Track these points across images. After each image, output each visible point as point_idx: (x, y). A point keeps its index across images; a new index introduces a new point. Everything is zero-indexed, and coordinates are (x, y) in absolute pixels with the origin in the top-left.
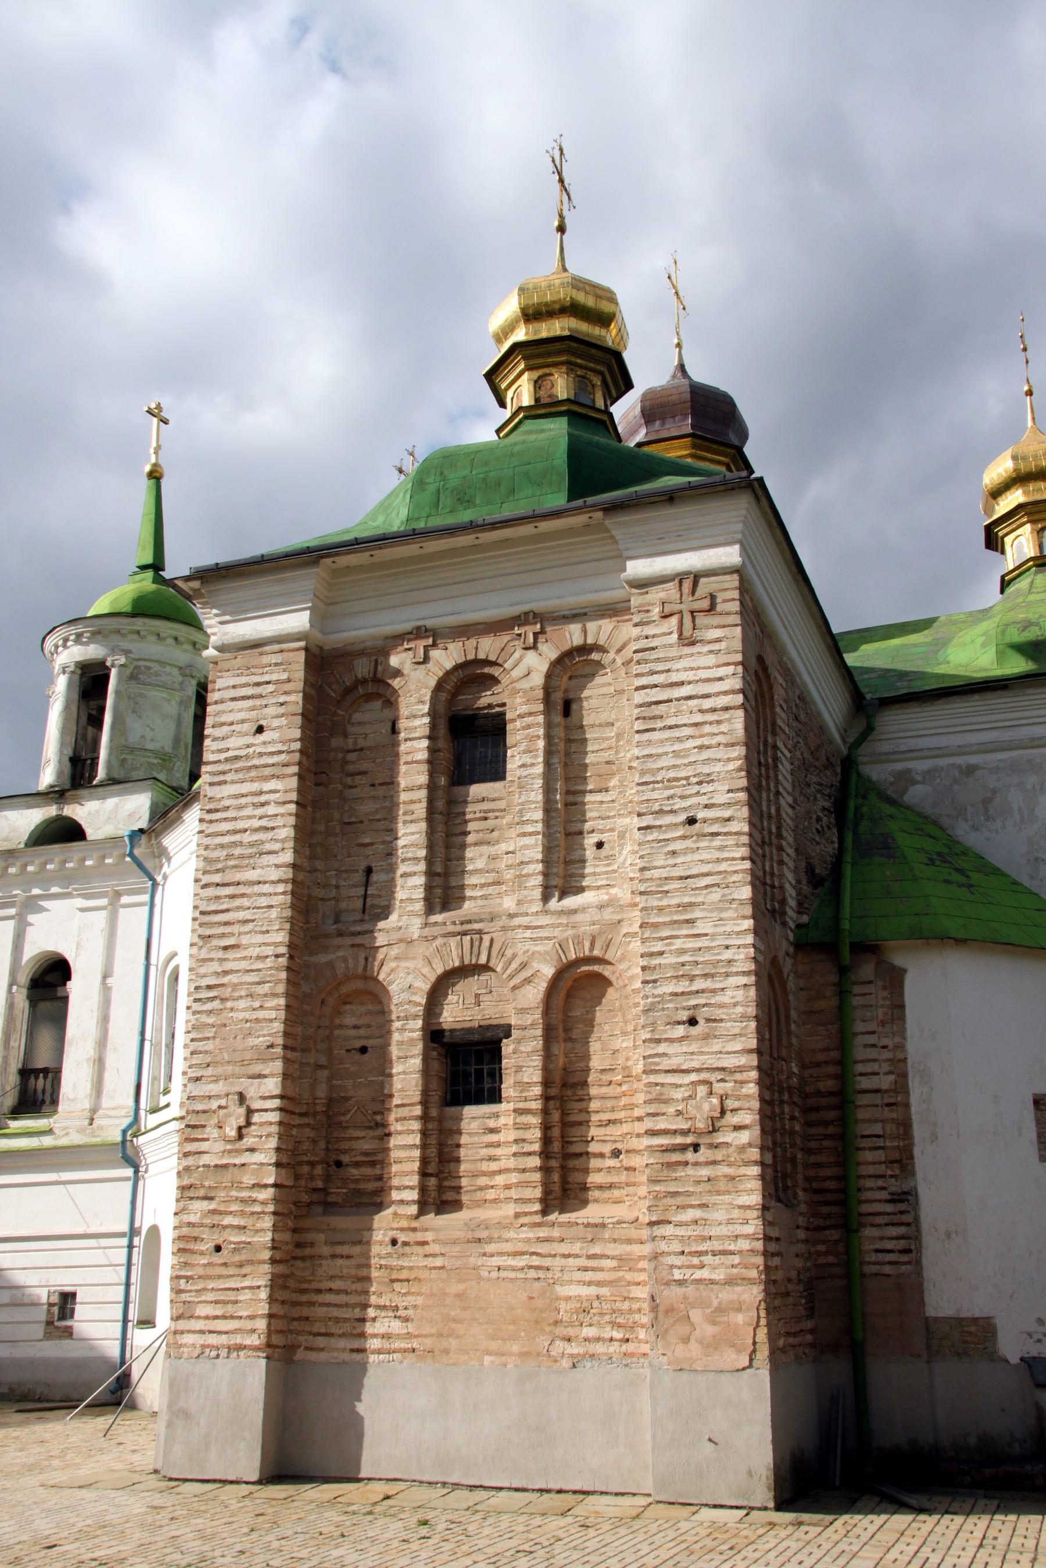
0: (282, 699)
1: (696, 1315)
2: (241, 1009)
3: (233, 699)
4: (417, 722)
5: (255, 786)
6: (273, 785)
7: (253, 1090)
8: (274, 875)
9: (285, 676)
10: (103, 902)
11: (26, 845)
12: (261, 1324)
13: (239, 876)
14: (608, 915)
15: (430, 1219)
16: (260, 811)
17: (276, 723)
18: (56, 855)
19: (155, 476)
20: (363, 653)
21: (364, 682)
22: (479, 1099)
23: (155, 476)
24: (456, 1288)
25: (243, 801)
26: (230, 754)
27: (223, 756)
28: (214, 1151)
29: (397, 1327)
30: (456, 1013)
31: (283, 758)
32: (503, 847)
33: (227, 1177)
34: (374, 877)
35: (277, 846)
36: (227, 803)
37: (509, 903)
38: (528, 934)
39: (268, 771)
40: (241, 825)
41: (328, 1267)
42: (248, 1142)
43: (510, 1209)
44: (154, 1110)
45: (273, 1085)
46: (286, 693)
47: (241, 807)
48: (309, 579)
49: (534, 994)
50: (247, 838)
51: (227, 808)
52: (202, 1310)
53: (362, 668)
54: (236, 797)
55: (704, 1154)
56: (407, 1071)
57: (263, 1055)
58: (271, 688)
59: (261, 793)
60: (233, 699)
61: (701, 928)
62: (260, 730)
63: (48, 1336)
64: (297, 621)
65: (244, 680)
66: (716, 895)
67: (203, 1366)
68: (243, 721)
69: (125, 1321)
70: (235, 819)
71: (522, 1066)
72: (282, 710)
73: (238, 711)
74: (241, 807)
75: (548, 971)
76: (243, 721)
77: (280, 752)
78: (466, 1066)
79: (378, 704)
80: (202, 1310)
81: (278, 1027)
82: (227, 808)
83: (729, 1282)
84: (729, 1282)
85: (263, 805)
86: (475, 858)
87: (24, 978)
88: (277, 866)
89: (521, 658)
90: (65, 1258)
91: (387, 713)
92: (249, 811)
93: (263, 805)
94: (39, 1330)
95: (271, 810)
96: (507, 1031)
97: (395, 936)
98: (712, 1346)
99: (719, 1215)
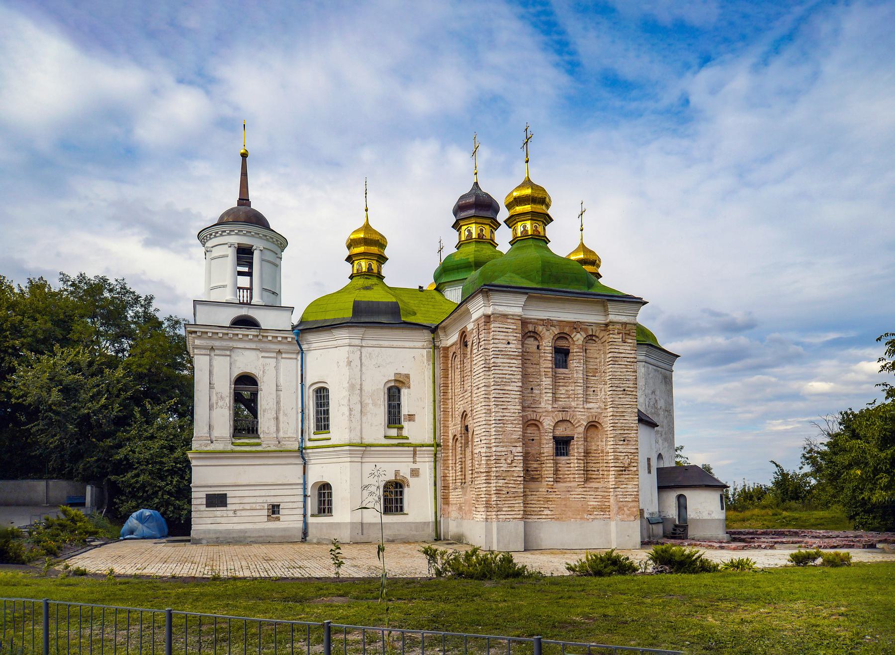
1: (625, 509)
2: (509, 427)
5: (508, 361)
6: (514, 361)
7: (514, 450)
8: (517, 389)
12: (522, 512)
13: (506, 388)
14: (599, 410)
15: (556, 485)
18: (252, 332)
20: (531, 323)
21: (530, 332)
22: (562, 454)
24: (564, 503)
28: (504, 467)
29: (549, 512)
30: (561, 432)
32: (570, 388)
33: (509, 474)
37: (573, 404)
40: (504, 372)
41: (530, 498)
42: (514, 464)
43: (576, 484)
44: (310, 440)
45: (520, 449)
48: (522, 299)
49: (581, 429)
50: (507, 376)
52: (504, 509)
53: (531, 328)
55: (627, 472)
56: (548, 448)
57: (517, 440)
61: (626, 418)
62: (509, 343)
63: (269, 520)
64: (518, 311)
66: (630, 410)
67: (506, 524)
69: (305, 516)
71: (577, 448)
73: (501, 336)
75: (585, 424)
78: (562, 445)
79: (532, 339)
80: (504, 509)
81: (520, 433)
83: (633, 501)
84: (633, 501)
86: (562, 390)
87: (233, 379)
90: (273, 493)
91: (536, 343)
94: (266, 519)
95: (514, 369)
96: (573, 438)
98: (629, 515)
99: (630, 486)
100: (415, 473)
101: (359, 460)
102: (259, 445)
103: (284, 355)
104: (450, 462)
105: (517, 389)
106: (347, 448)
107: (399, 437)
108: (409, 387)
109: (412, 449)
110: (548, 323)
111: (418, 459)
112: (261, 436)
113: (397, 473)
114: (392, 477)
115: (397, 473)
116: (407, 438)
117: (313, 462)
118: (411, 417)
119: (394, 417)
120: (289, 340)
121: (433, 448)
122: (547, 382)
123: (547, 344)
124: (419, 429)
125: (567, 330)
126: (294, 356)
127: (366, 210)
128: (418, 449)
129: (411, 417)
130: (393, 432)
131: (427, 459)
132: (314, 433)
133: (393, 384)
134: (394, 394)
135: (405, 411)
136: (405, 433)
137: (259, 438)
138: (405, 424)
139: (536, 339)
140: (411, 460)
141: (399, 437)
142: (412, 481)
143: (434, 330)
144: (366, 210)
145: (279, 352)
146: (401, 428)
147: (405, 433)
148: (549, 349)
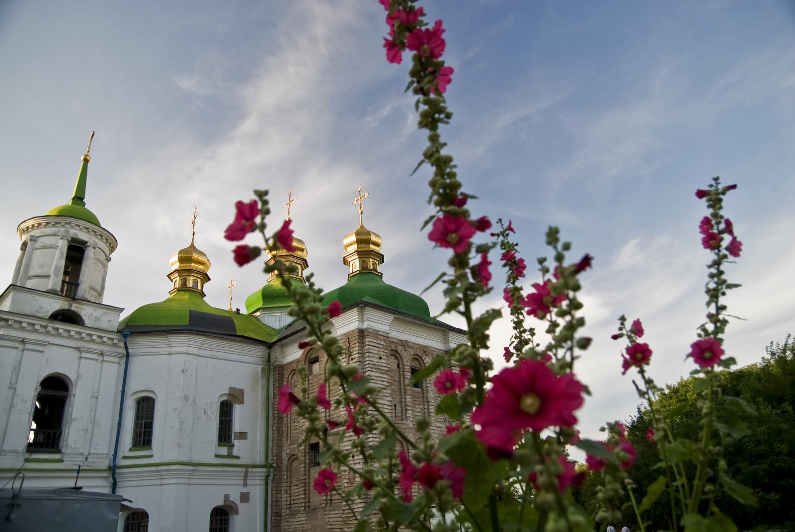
0: (385, 351)
3: (372, 346)
4: (407, 367)
6: (385, 376)
8: (388, 403)
9: (385, 344)
10: (95, 356)
11: (49, 318)
16: (382, 383)
17: (384, 357)
18: (74, 329)
19: (86, 161)
23: (86, 161)
25: (379, 378)
26: (373, 363)
27: (372, 363)
31: (387, 369)
34: (397, 408)
35: (388, 395)
36: (375, 378)
38: (433, 431)
39: (383, 372)
44: (125, 458)
46: (386, 349)
47: (378, 380)
51: (374, 380)
54: (376, 377)
58: (381, 346)
59: (382, 377)
60: (372, 346)
65: (374, 341)
68: (376, 354)
70: (376, 383)
72: (385, 354)
73: (374, 350)
74: (378, 380)
76: (376, 354)
77: (386, 367)
82: (374, 380)
85: (383, 381)
88: (388, 401)
89: (425, 358)
91: (396, 361)
92: (380, 382)
93: (383, 381)
97: (407, 426)
100: (245, 497)
101: (186, 481)
102: (61, 461)
103: (106, 358)
104: (284, 485)
105: (388, 403)
106: (176, 467)
107: (230, 456)
108: (243, 403)
109: (244, 469)
110: (405, 344)
111: (248, 482)
112: (63, 451)
113: (226, 497)
114: (220, 502)
115: (226, 497)
116: (238, 457)
117: (126, 484)
118: (242, 436)
119: (225, 435)
120: (115, 341)
121: (265, 470)
122: (408, 398)
123: (407, 364)
124: (250, 448)
125: (419, 353)
126: (117, 360)
127: (194, 234)
128: (250, 470)
129: (242, 436)
130: (224, 451)
131: (257, 482)
132: (130, 450)
133: (225, 398)
134: (226, 410)
135: (237, 427)
136: (235, 452)
137: (59, 452)
138: (236, 442)
139: (396, 358)
140: (242, 482)
141: (230, 456)
142: (242, 507)
143: (270, 346)
144: (194, 234)
145: (102, 354)
146: (232, 446)
147: (235, 452)
148: (408, 368)
